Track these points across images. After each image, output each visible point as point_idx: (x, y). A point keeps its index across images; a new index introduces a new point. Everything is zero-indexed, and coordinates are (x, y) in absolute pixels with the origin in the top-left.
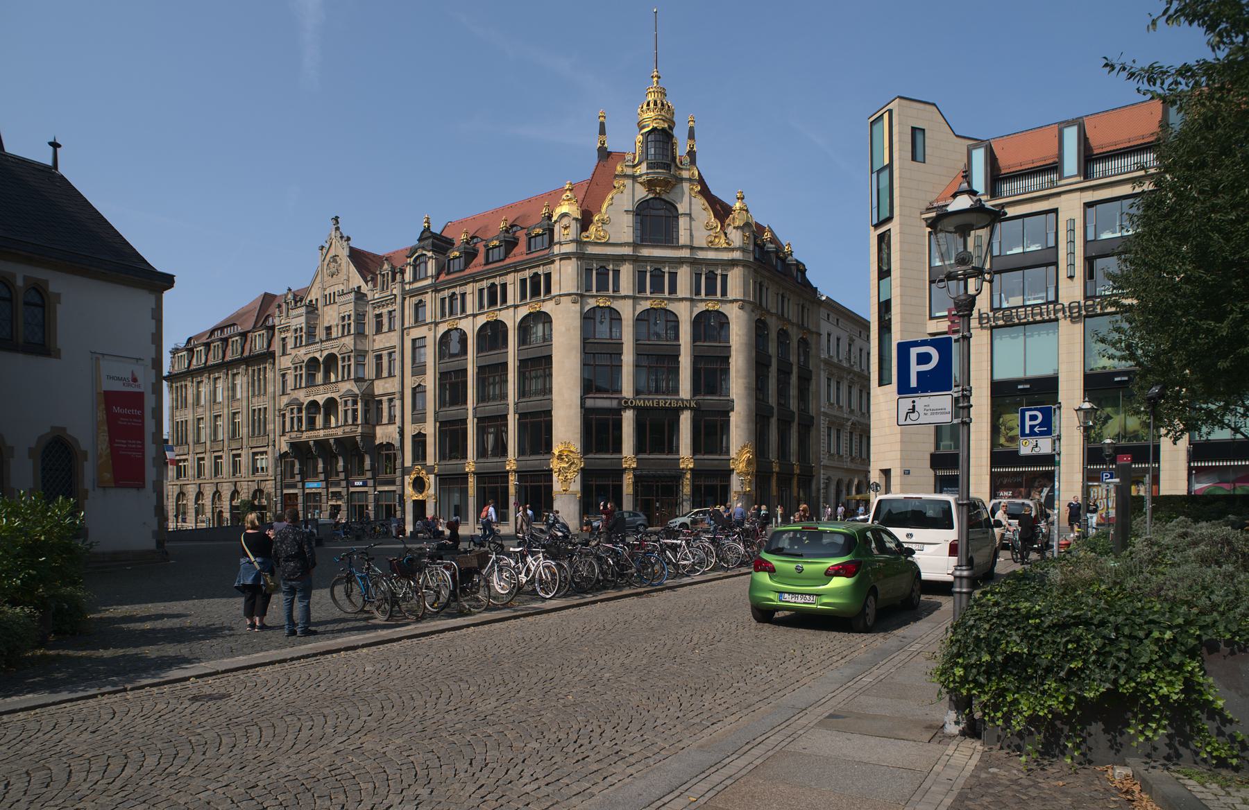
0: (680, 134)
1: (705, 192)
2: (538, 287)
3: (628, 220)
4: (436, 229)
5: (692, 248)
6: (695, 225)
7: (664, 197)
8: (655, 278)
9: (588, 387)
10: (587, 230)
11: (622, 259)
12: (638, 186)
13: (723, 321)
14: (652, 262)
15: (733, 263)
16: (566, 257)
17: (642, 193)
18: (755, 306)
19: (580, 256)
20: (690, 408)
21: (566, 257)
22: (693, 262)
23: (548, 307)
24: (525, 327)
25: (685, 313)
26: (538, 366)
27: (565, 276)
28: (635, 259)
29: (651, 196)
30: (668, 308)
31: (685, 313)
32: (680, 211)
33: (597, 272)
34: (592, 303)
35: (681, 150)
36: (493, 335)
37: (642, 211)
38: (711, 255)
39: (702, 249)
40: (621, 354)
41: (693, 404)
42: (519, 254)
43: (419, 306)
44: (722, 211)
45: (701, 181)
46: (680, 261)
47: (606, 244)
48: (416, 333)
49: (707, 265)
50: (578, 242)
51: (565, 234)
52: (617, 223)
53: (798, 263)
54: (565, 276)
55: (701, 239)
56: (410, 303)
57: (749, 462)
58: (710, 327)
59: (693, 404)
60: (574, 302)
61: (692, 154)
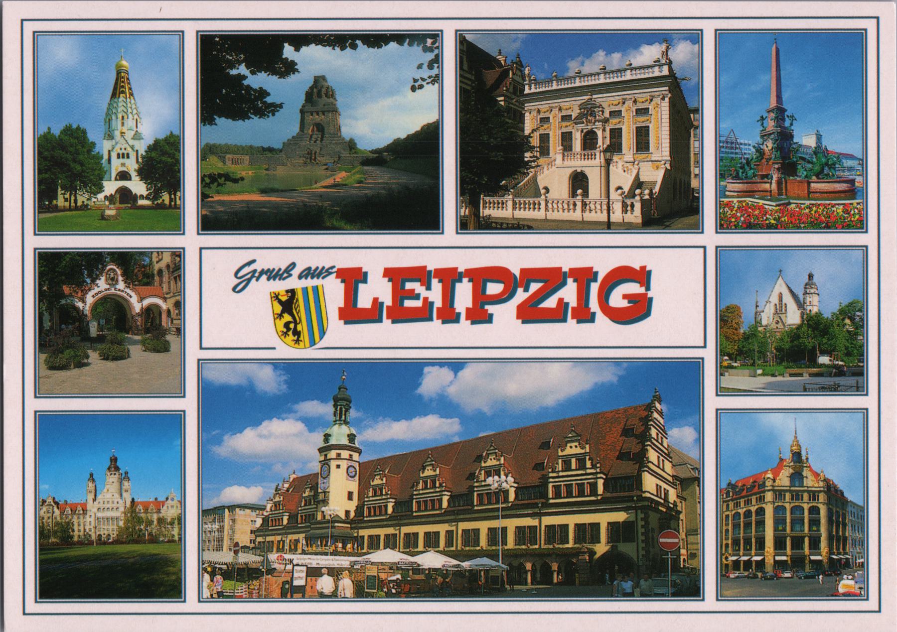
0: (803, 453)
1: (811, 470)
2: (761, 499)
3: (788, 479)
4: (733, 482)
6: (810, 482)
8: (796, 496)
9: (776, 529)
15: (821, 491)
16: (769, 490)
17: (791, 471)
18: (828, 503)
19: (774, 491)
21: (769, 490)
22: (809, 492)
23: (764, 506)
24: (757, 512)
25: (806, 507)
26: (761, 523)
27: (769, 496)
28: (790, 491)
31: (806, 507)
33: (779, 494)
34: (776, 504)
35: (804, 458)
36: (748, 514)
37: (792, 477)
42: (756, 490)
43: (728, 505)
44: (816, 475)
45: (809, 467)
48: (727, 513)
50: (773, 486)
51: (769, 483)
52: (784, 480)
53: (841, 491)
54: (769, 496)
55: (810, 484)
56: (725, 504)
58: (814, 510)
61: (807, 459)
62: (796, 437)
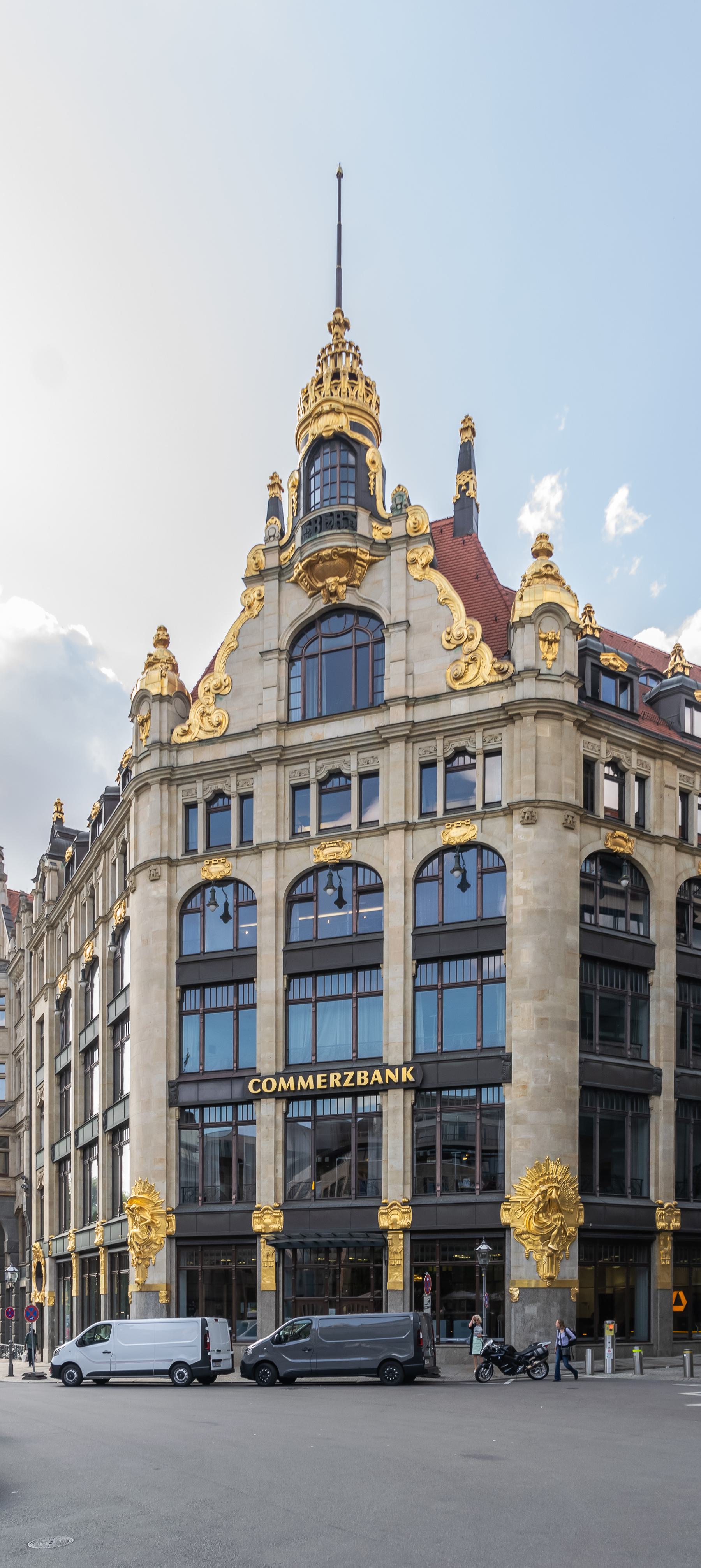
3: (274, 670)
5: (411, 702)
7: (350, 599)
10: (184, 718)
11: (250, 763)
12: (289, 589)
13: (488, 862)
14: (319, 756)
15: (509, 714)
20: (406, 1086)
22: (413, 733)
29: (321, 604)
30: (354, 856)
31: (393, 859)
32: (386, 622)
38: (459, 706)
39: (434, 698)
40: (251, 980)
41: (407, 1075)
46: (381, 739)
47: (225, 738)
49: (448, 734)
55: (433, 676)
57: (548, 1206)
59: (407, 1075)
60: (155, 879)
62: (340, 324)
